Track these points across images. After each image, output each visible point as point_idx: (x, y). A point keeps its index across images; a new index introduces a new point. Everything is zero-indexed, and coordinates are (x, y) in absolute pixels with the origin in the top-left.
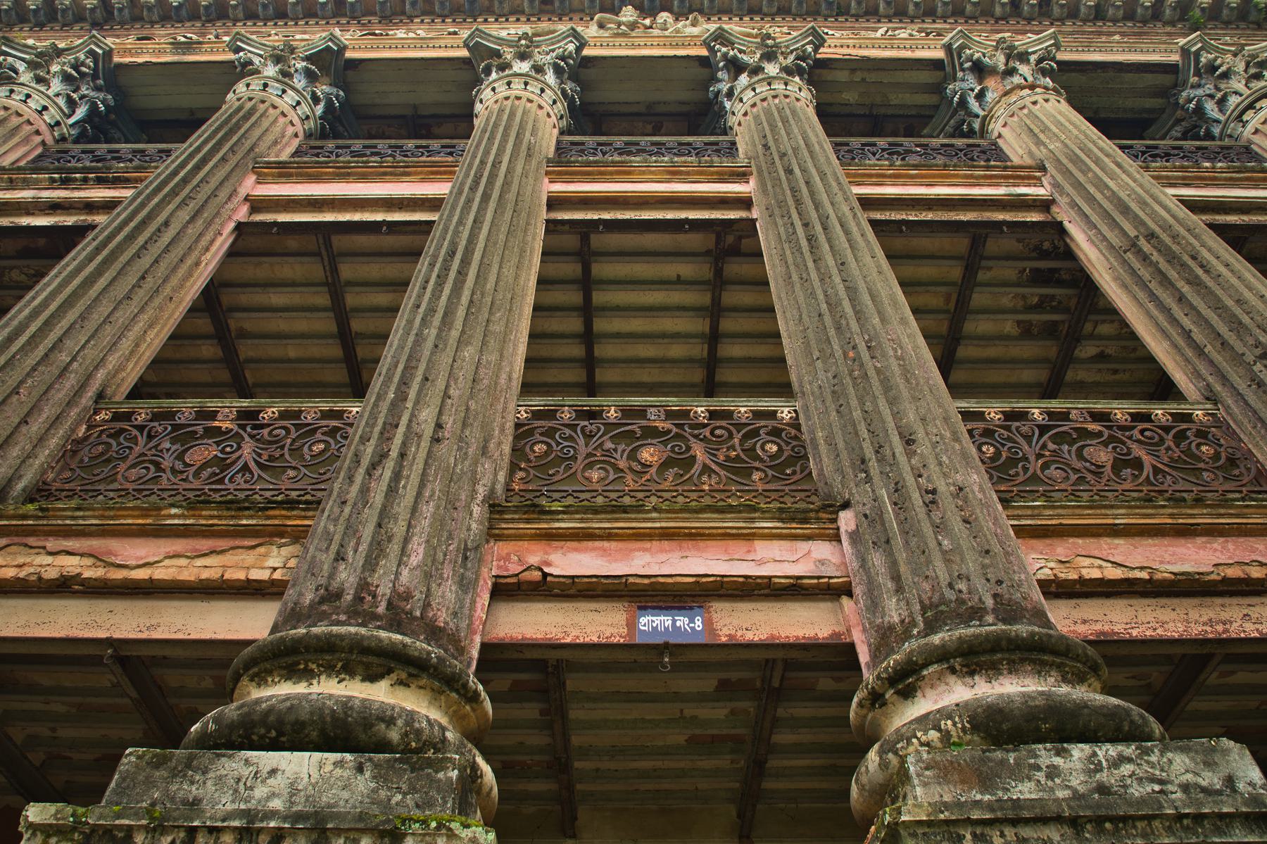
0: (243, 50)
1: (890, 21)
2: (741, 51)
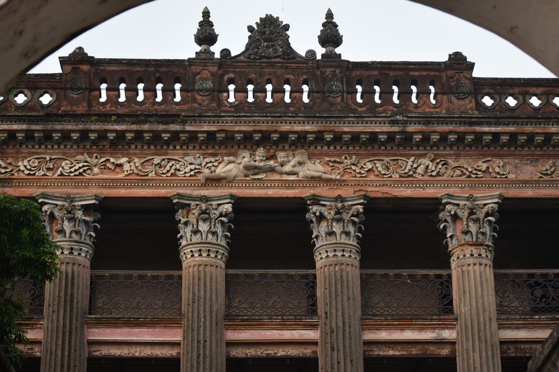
0: (47, 203)
1: (418, 149)
2: (324, 205)
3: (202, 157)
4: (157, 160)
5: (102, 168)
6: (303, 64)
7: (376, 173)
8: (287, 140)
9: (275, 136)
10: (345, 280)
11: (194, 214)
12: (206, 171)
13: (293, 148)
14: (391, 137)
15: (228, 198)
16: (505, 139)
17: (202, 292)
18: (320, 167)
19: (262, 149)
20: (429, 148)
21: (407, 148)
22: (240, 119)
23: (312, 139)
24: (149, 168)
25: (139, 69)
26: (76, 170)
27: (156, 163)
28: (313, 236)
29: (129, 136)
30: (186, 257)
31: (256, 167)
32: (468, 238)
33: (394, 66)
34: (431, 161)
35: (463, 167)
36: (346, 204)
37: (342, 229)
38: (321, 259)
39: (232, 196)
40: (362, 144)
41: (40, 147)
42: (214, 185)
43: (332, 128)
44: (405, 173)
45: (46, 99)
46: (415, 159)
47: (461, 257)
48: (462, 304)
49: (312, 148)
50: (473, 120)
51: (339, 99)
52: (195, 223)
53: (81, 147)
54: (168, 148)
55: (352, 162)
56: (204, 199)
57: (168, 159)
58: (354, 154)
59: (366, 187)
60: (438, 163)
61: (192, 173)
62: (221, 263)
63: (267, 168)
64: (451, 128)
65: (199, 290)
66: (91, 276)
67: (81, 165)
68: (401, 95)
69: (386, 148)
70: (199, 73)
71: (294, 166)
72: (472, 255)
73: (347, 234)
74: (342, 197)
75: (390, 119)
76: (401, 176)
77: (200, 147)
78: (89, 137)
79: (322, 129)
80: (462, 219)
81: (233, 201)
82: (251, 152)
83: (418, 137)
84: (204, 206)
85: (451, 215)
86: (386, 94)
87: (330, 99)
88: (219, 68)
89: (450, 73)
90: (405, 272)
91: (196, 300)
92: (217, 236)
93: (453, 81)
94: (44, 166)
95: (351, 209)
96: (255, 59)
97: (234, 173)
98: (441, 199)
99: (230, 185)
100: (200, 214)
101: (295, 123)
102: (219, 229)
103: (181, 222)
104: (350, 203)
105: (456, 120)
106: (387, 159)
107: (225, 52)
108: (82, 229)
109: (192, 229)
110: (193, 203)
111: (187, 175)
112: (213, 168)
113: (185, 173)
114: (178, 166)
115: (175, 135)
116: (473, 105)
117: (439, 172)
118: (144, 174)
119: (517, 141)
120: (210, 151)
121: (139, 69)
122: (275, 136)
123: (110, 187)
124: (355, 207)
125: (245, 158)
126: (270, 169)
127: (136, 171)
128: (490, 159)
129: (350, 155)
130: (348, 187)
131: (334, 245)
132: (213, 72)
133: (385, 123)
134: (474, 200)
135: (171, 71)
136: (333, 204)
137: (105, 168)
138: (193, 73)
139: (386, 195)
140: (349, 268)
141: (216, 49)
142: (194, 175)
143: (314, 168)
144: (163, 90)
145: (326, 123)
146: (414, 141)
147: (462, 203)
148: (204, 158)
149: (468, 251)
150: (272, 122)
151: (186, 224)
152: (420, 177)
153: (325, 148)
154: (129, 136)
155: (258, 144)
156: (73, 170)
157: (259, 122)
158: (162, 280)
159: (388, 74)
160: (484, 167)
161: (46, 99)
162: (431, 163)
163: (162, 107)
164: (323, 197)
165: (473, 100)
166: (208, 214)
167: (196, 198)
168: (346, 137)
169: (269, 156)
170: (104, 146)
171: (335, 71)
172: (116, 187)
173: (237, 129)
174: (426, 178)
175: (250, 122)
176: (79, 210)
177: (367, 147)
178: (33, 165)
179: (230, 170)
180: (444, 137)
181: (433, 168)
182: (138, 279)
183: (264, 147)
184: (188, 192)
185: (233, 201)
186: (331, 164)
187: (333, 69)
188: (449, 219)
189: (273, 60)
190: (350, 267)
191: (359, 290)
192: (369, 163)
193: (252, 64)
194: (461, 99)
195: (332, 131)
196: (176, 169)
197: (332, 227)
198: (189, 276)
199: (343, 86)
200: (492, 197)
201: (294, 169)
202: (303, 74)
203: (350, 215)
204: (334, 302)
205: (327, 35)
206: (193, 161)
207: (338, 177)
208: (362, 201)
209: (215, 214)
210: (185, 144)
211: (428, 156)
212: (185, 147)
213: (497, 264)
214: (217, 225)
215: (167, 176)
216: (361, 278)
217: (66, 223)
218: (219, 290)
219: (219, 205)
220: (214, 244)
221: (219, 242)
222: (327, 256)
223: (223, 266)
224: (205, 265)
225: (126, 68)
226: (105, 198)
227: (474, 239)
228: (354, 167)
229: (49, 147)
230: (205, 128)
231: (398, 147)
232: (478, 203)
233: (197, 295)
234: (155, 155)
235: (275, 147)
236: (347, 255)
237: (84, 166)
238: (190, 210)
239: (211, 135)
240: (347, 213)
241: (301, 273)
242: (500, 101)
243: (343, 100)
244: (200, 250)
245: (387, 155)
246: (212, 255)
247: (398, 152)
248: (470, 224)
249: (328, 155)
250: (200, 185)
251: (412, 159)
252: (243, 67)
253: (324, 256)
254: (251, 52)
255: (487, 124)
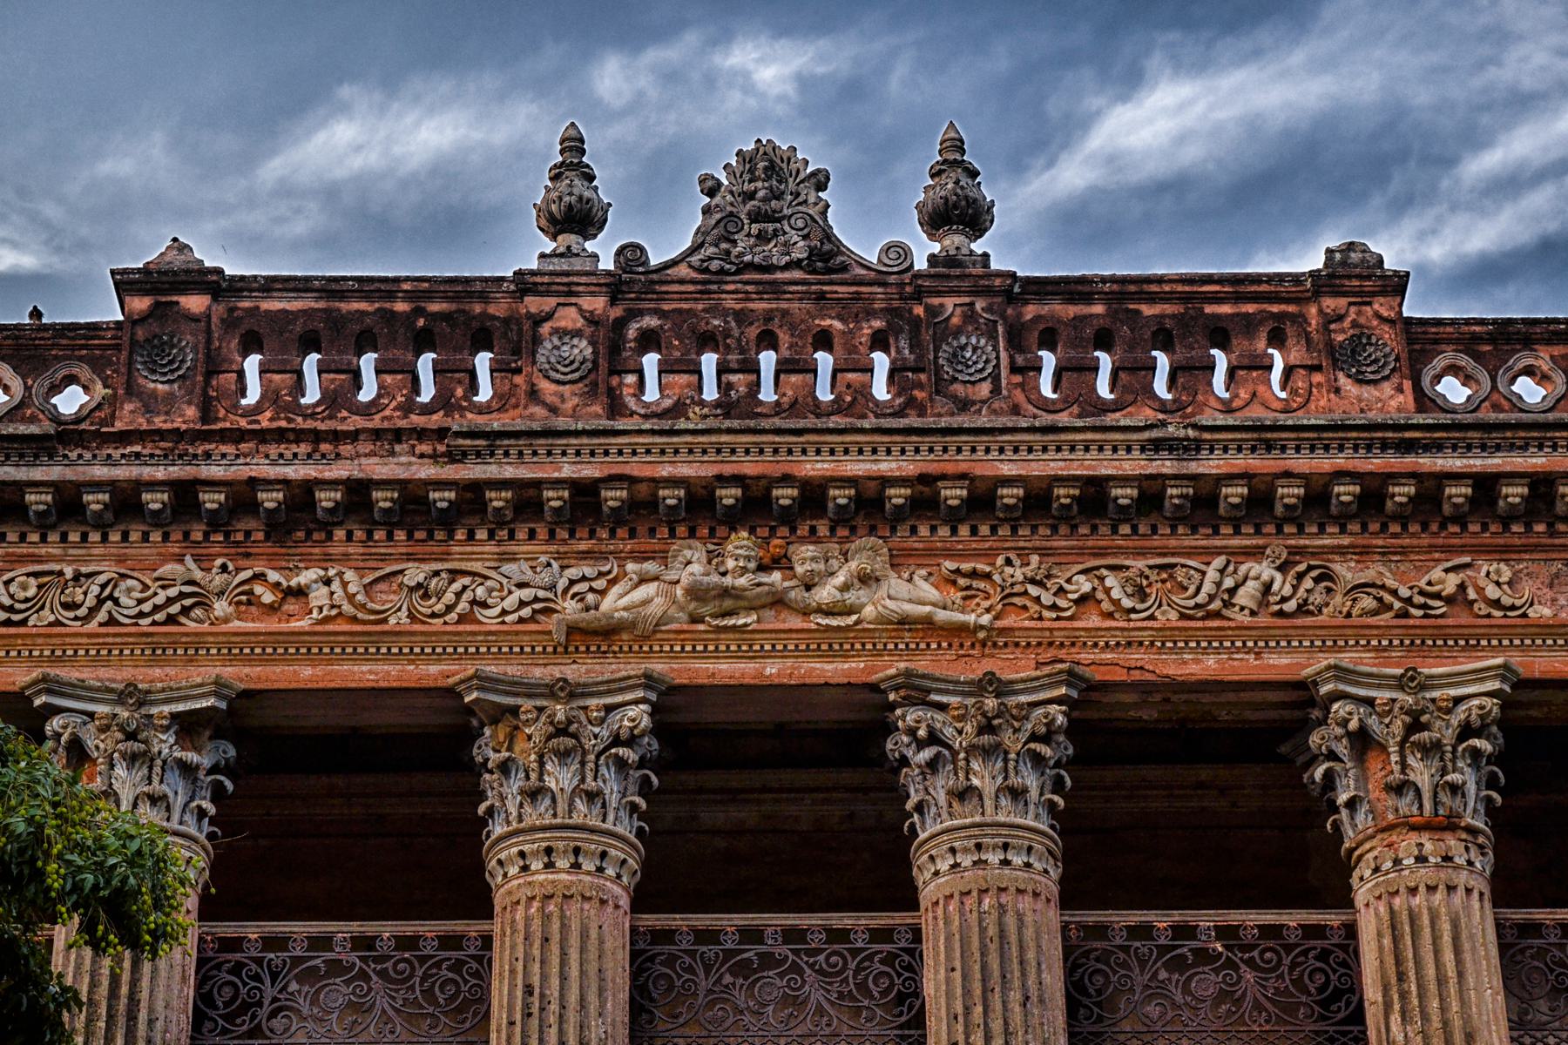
0: (60, 710)
1: (1237, 532)
2: (942, 707)
3: (555, 565)
4: (415, 574)
5: (239, 603)
6: (870, 284)
7: (1106, 606)
8: (825, 508)
9: (785, 495)
10: (1013, 938)
11: (530, 737)
12: (570, 607)
13: (842, 532)
14: (1150, 494)
15: (639, 685)
16: (1514, 493)
17: (555, 982)
18: (928, 591)
19: (745, 534)
20: (1270, 529)
21: (1203, 530)
22: (675, 439)
23: (901, 501)
24: (386, 598)
25: (363, 306)
26: (157, 609)
27: (413, 584)
28: (909, 805)
29: (326, 499)
30: (505, 875)
31: (726, 592)
32: (1406, 804)
33: (1154, 288)
34: (1279, 569)
35: (1383, 587)
36: (1012, 701)
37: (1000, 780)
38: (935, 876)
39: (649, 681)
40: (1060, 518)
41: (44, 539)
42: (593, 648)
43: (963, 467)
44: (1197, 606)
45: (70, 401)
46: (1228, 562)
47: (1389, 864)
48: (1395, 1018)
49: (903, 530)
50: (1408, 435)
51: (985, 389)
52: (534, 765)
53: (176, 536)
54: (451, 536)
55: (1029, 574)
56: (562, 689)
57: (450, 571)
58: (1035, 550)
59: (1073, 650)
60: (1300, 577)
61: (526, 612)
62: (617, 890)
63: (758, 596)
64: (1340, 461)
65: (544, 977)
66: (200, 939)
67: (172, 592)
68: (1179, 374)
69: (1135, 529)
70: (549, 316)
71: (845, 588)
72: (1422, 859)
73: (1017, 794)
74: (999, 680)
75: (1146, 435)
76: (1183, 617)
77: (552, 534)
78: (198, 505)
79: (933, 468)
80: (1383, 748)
81: (653, 697)
82: (712, 547)
83: (1235, 493)
84: (560, 711)
85: (1348, 734)
86: (1134, 374)
87: (958, 389)
88: (613, 301)
89: (1330, 303)
90: (1206, 919)
91: (535, 1009)
92: (604, 806)
93: (1343, 331)
94: (54, 596)
95: (1026, 718)
96: (722, 271)
97: (657, 608)
98: (1315, 683)
99: (646, 648)
100: (549, 738)
101: (846, 452)
102: (611, 786)
103: (490, 765)
104: (1023, 699)
105: (1354, 435)
106: (1140, 564)
107: (631, 255)
108: (175, 788)
109: (521, 783)
110: (527, 704)
111: (508, 619)
112: (590, 597)
113: (504, 612)
114: (480, 591)
115: (468, 495)
116: (1407, 399)
117: (1306, 601)
118: (372, 617)
119: (1552, 503)
120: (583, 546)
121: (363, 306)
122: (785, 495)
123: (264, 660)
124: (1040, 711)
125: (692, 564)
126: (770, 600)
127: (347, 608)
128: (1467, 559)
129: (1023, 553)
130: (1018, 651)
131: (976, 831)
132: (591, 312)
133: (1129, 450)
134: (1423, 687)
135: (464, 311)
136: (970, 701)
137: (249, 603)
138: (529, 315)
139: (1137, 675)
140: (1025, 903)
141: (604, 250)
142: (532, 619)
143: (913, 593)
144: (438, 371)
145: (945, 450)
146: (1222, 505)
147: (1382, 695)
148: (563, 568)
149: (1407, 844)
150: (776, 451)
151: (505, 768)
152: (1245, 619)
153: (944, 531)
154: (326, 499)
155: (734, 519)
156: (147, 607)
157: (733, 451)
158: (428, 951)
159: (1138, 312)
160: (1451, 583)
161: (70, 401)
162: (1278, 577)
163: (435, 417)
164: (938, 680)
165: (1407, 385)
166: (575, 736)
167: (538, 686)
168: (1010, 495)
169: (766, 561)
170: (248, 534)
171: (972, 304)
172: (285, 659)
173: (665, 471)
174: (1263, 620)
175: (704, 452)
176: (166, 729)
177: (1074, 528)
178: (21, 595)
179: (646, 602)
180: (1317, 498)
181: (1287, 590)
182: (353, 950)
183: (752, 531)
184: (513, 670)
185: (653, 697)
186: (962, 582)
187: (967, 300)
188: (1342, 749)
189: (779, 275)
190: (1028, 899)
191: (1059, 972)
192: (1082, 578)
193: (714, 287)
194: (1369, 382)
195: (963, 476)
196: (474, 602)
197: (967, 773)
198: (514, 931)
199: (996, 348)
200: (1479, 675)
201: (846, 596)
202: (870, 314)
203: (1023, 737)
204: (979, 1009)
205: (946, 199)
206: (529, 575)
207: (986, 619)
208: (1063, 690)
209: (596, 737)
210: (500, 525)
211: (1268, 551)
212: (504, 533)
213: (1504, 890)
214: (603, 770)
215: (445, 623)
216: (1065, 938)
217: (120, 771)
218: (609, 975)
219: (609, 709)
220: (593, 831)
221: (608, 826)
222: (955, 865)
223: (625, 902)
224: (565, 896)
225: (321, 305)
226: (246, 694)
227: (1428, 806)
228: (1034, 591)
229: (74, 537)
230: (567, 471)
231: (1174, 528)
232: (1436, 694)
233: (537, 991)
234: (408, 560)
235: (784, 531)
236: (1018, 860)
237: (182, 596)
238: (516, 728)
239: (584, 493)
240: (1016, 731)
241: (874, 923)
242: (1494, 387)
243: (996, 390)
244: (549, 851)
245: (1141, 553)
246: (588, 865)
247: (1173, 542)
248: (1411, 761)
249: (950, 554)
250: (550, 649)
251: (1219, 562)
252: (684, 297)
253: (943, 866)
254: (711, 250)
255: (1455, 448)
